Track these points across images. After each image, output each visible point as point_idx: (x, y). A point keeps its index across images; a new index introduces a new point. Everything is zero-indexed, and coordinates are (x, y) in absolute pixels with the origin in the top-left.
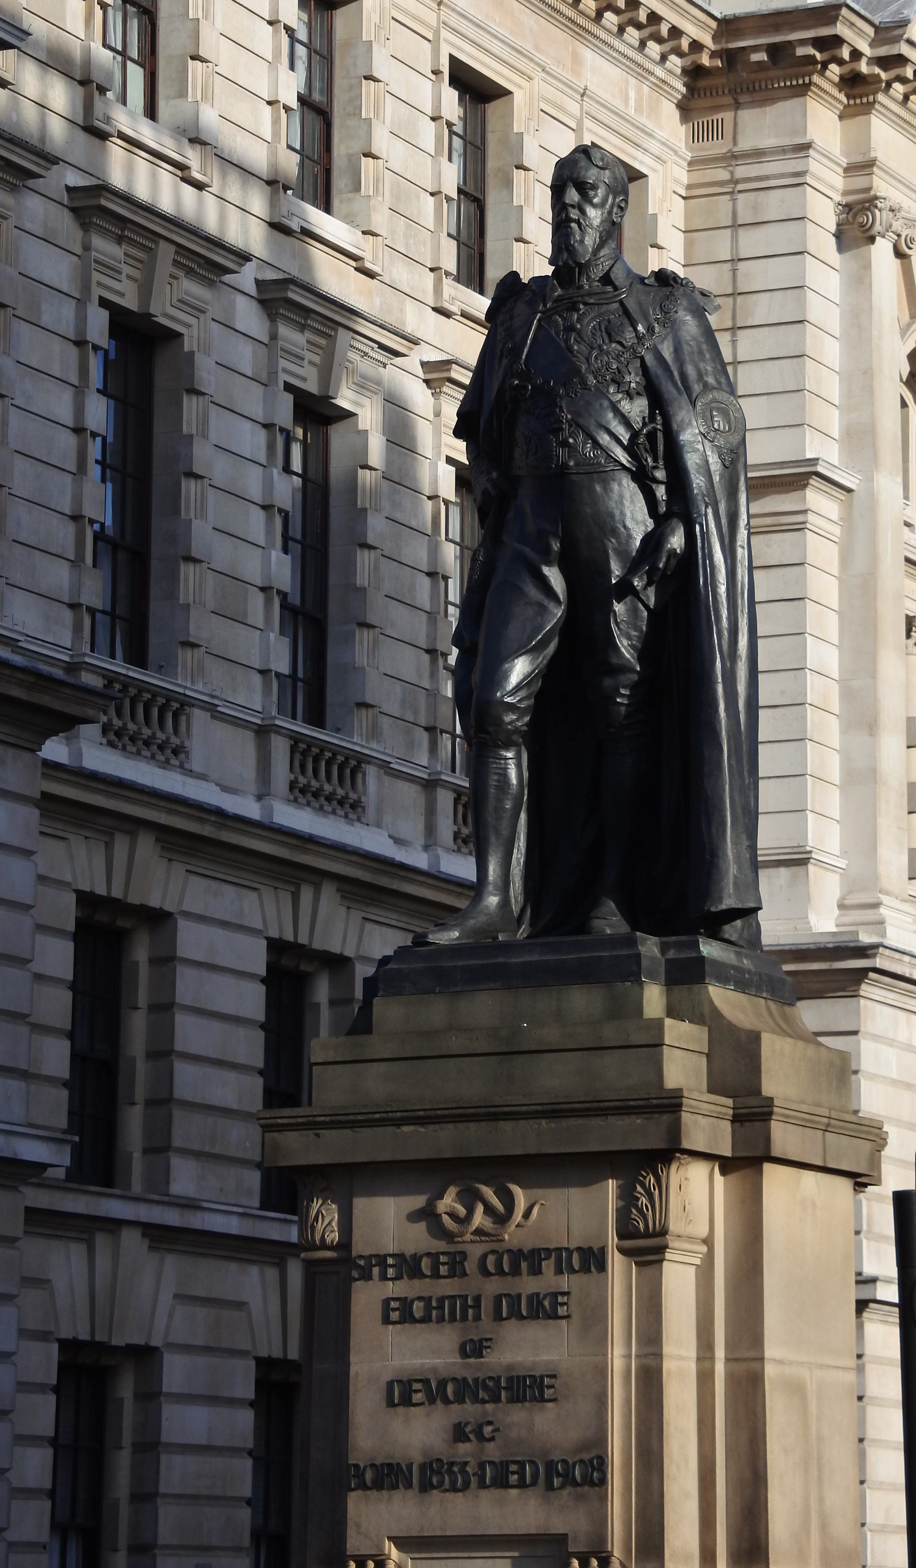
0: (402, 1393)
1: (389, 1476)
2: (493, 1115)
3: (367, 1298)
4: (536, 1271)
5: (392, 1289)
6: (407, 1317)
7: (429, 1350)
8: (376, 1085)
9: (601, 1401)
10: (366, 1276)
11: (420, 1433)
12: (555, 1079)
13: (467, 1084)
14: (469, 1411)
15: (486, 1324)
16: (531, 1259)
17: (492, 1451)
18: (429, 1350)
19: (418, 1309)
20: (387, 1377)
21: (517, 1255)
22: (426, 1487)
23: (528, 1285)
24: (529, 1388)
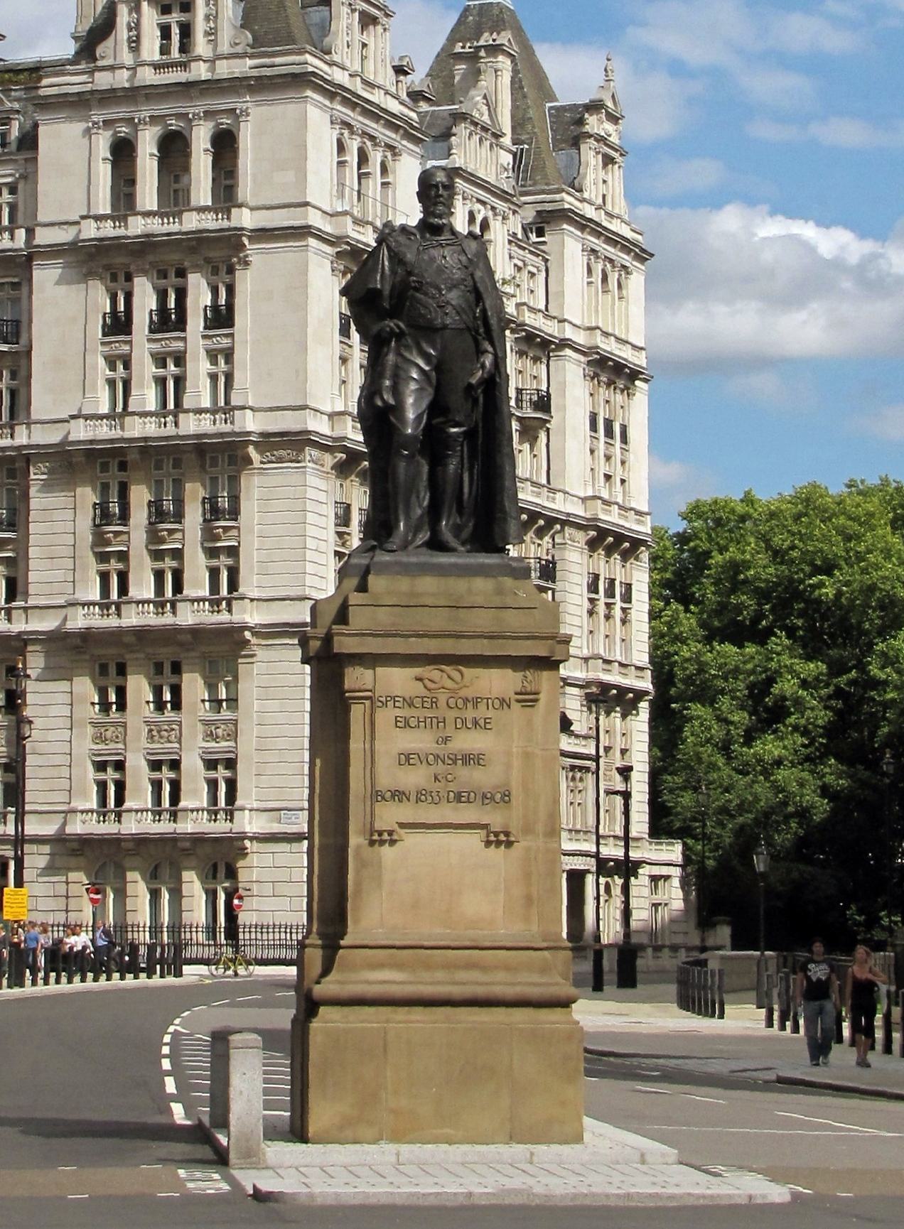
0: (407, 759)
1: (398, 795)
2: (458, 636)
3: (385, 717)
4: (475, 706)
5: (398, 712)
6: (407, 724)
7: (420, 741)
8: (384, 618)
9: (508, 766)
10: (385, 704)
11: (414, 778)
12: (481, 621)
13: (438, 621)
14: (440, 768)
15: (450, 731)
16: (476, 702)
17: (452, 786)
18: (420, 741)
19: (413, 722)
20: (395, 752)
21: (466, 700)
22: (418, 800)
23: (470, 714)
24: (470, 759)
